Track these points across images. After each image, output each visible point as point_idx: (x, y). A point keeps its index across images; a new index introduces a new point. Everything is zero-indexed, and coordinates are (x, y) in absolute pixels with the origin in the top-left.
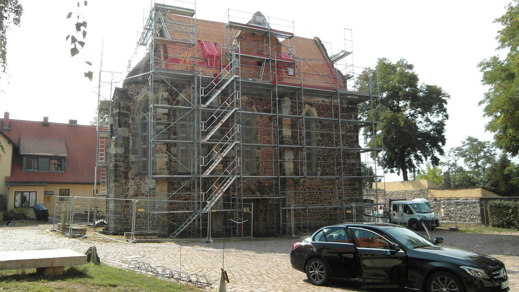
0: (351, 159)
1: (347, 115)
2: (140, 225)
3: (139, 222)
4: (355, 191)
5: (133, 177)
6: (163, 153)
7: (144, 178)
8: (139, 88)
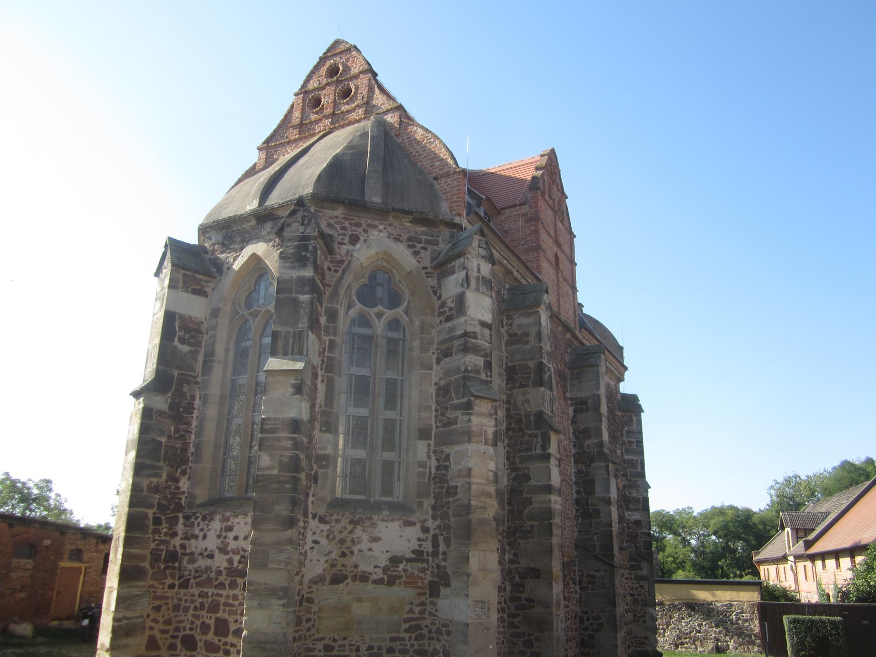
0: (631, 510)
1: (624, 416)
4: (641, 583)
5: (322, 511)
6: (486, 443)
7: (370, 519)
8: (358, 225)
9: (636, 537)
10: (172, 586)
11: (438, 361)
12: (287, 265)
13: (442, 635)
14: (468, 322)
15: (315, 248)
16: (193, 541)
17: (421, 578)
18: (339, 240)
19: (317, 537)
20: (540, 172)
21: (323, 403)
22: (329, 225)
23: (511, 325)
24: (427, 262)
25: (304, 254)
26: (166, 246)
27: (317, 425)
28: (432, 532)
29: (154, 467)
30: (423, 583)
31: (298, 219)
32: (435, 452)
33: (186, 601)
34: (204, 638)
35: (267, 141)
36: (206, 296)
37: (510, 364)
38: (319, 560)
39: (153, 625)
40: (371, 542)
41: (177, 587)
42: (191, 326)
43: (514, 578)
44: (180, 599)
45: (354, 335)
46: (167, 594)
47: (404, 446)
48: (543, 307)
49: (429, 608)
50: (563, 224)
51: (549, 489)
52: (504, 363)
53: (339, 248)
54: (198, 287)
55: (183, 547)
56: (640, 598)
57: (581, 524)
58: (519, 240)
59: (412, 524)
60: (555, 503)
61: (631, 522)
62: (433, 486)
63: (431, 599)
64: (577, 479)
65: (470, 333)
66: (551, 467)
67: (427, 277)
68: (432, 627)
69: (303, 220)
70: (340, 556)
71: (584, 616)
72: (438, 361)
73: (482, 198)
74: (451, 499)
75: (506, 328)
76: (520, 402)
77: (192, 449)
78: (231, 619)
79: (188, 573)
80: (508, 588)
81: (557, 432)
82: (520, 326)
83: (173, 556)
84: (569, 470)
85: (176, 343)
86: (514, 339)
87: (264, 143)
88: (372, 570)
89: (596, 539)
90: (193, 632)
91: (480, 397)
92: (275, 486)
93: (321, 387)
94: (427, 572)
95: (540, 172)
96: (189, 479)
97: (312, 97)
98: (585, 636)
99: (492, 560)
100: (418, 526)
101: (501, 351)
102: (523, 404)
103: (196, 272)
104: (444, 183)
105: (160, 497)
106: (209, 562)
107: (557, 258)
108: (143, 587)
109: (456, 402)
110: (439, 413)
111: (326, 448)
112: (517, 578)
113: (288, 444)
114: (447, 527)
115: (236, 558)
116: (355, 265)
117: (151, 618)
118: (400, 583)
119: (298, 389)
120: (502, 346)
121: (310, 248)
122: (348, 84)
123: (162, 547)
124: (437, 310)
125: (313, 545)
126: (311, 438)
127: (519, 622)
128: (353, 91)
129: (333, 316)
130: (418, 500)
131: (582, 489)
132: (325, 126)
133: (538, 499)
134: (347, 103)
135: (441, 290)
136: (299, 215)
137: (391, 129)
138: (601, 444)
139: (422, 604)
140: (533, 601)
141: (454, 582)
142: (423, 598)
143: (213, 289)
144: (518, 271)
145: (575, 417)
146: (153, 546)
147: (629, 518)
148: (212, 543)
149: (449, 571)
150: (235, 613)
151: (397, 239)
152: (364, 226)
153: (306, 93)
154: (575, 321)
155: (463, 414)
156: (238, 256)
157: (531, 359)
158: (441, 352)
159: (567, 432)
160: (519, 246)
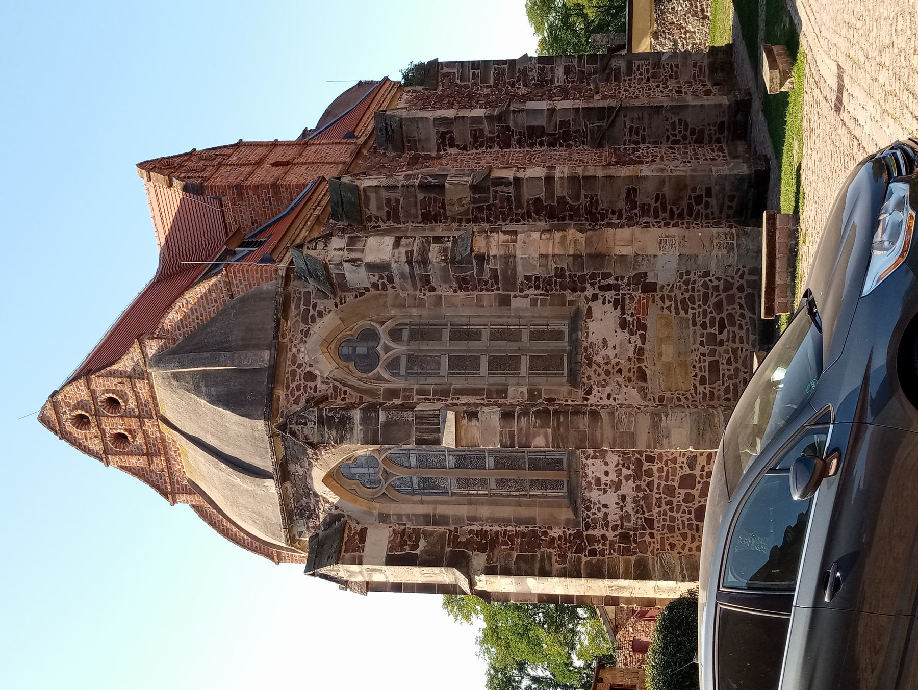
0: (553, 77)
2: (739, 365)
3: (732, 368)
4: (635, 68)
5: (581, 393)
6: (515, 241)
7: (586, 349)
8: (293, 373)
9: (583, 72)
10: (652, 536)
11: (433, 289)
12: (348, 436)
13: (690, 279)
14: (397, 260)
15: (331, 410)
16: (610, 518)
17: (639, 300)
18: (312, 391)
19: (605, 396)
20: (176, 182)
21: (479, 397)
22: (296, 402)
23: (377, 218)
24: (330, 303)
25: (337, 420)
26: (313, 575)
27: (501, 401)
28: (597, 291)
29: (542, 559)
30: (643, 299)
31: (300, 429)
32: (522, 290)
33: (665, 520)
34: (697, 499)
35: (165, 494)
36: (366, 529)
37: (420, 219)
38: (625, 393)
39: (687, 548)
40: (607, 347)
41: (652, 531)
42: (398, 540)
43: (636, 214)
44: (663, 526)
45: (408, 373)
46: (659, 539)
47: (516, 321)
48: (357, 183)
49: (666, 293)
50: (230, 156)
51: (549, 179)
52: (418, 225)
53: (320, 391)
54: (357, 537)
55: (615, 528)
56: (651, 71)
57: (576, 142)
58: (264, 208)
59: (590, 309)
60: (563, 173)
61: (566, 79)
62: (554, 292)
63: (658, 290)
64: (528, 146)
65: (407, 257)
66: (527, 177)
67: (345, 302)
68: (683, 289)
69: (301, 424)
70: (621, 374)
71: (671, 140)
72: (433, 289)
73: (227, 249)
74: (567, 273)
75: (381, 223)
76: (460, 208)
77: (522, 528)
78: (680, 473)
79: (639, 520)
80: (646, 219)
81: (490, 170)
82: (379, 208)
83: (624, 537)
84: (518, 154)
85: (418, 552)
86: (393, 214)
87: (167, 498)
88: (634, 345)
89: (591, 125)
90: (693, 510)
91: (472, 246)
92: (562, 430)
93: (464, 400)
94: (633, 295)
95: (176, 182)
96: (551, 528)
97: (113, 444)
98: (692, 138)
99: (624, 233)
100: (590, 304)
101: (408, 227)
102: (463, 206)
103: (342, 541)
104: (238, 287)
105: (569, 552)
106: (629, 500)
107: (276, 164)
108: (654, 559)
109: (475, 271)
110: (485, 287)
111: (522, 392)
112: (637, 211)
113: (524, 420)
114: (593, 276)
115: (625, 472)
116: (338, 374)
117: (681, 551)
118: (644, 319)
119: (473, 415)
120: (401, 228)
121: (331, 414)
122: (101, 402)
123: (616, 546)
124: (379, 292)
125: (612, 398)
126: (514, 406)
127: (678, 208)
128: (111, 395)
129: (393, 393)
130: (567, 305)
131: (538, 140)
132: (153, 426)
133: (560, 190)
134: (126, 402)
135: (359, 289)
136: (295, 428)
137: (166, 348)
138: (490, 118)
139: (662, 298)
140: (658, 195)
141: (643, 269)
142: (657, 298)
143: (358, 523)
144: (314, 210)
145: (458, 147)
146: (615, 555)
147: (561, 80)
148: (611, 498)
149: (633, 273)
151: (307, 333)
152: (294, 367)
153: (106, 452)
154: (346, 143)
155: (488, 264)
156: (324, 498)
157: (415, 196)
158: (424, 287)
159: (477, 156)
160: (272, 208)
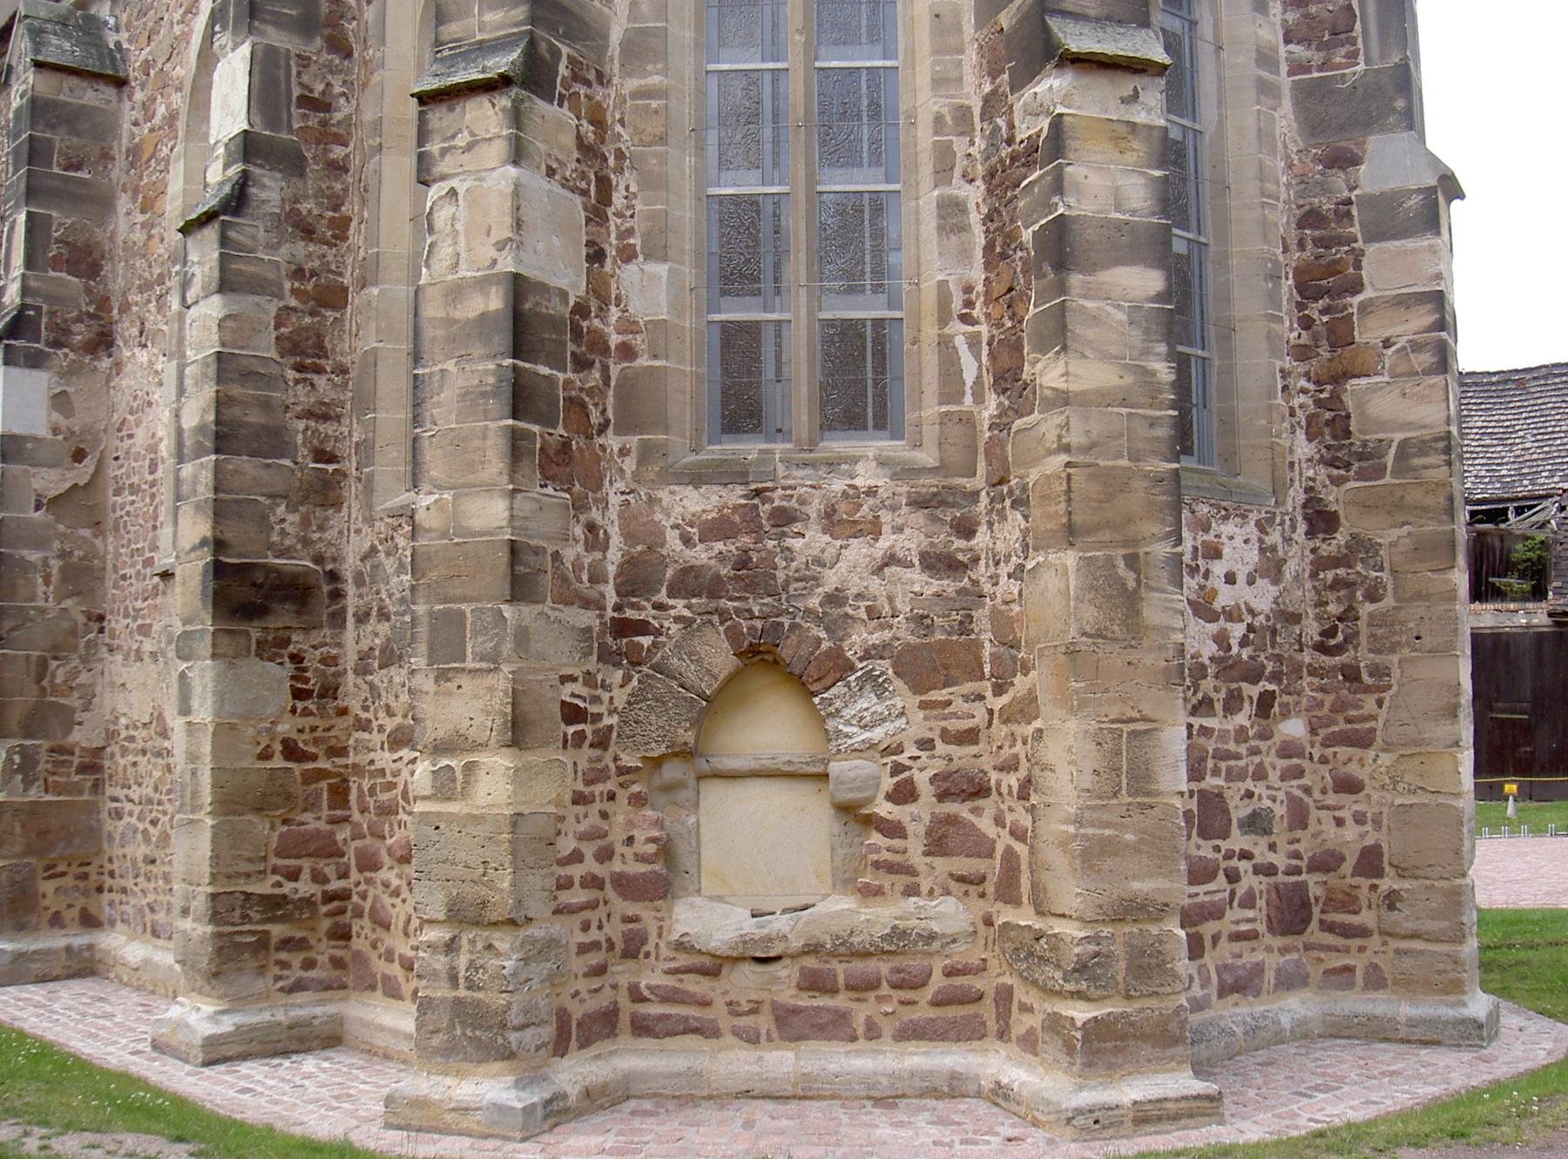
115: (1237, 630)
150: (1241, 775)
